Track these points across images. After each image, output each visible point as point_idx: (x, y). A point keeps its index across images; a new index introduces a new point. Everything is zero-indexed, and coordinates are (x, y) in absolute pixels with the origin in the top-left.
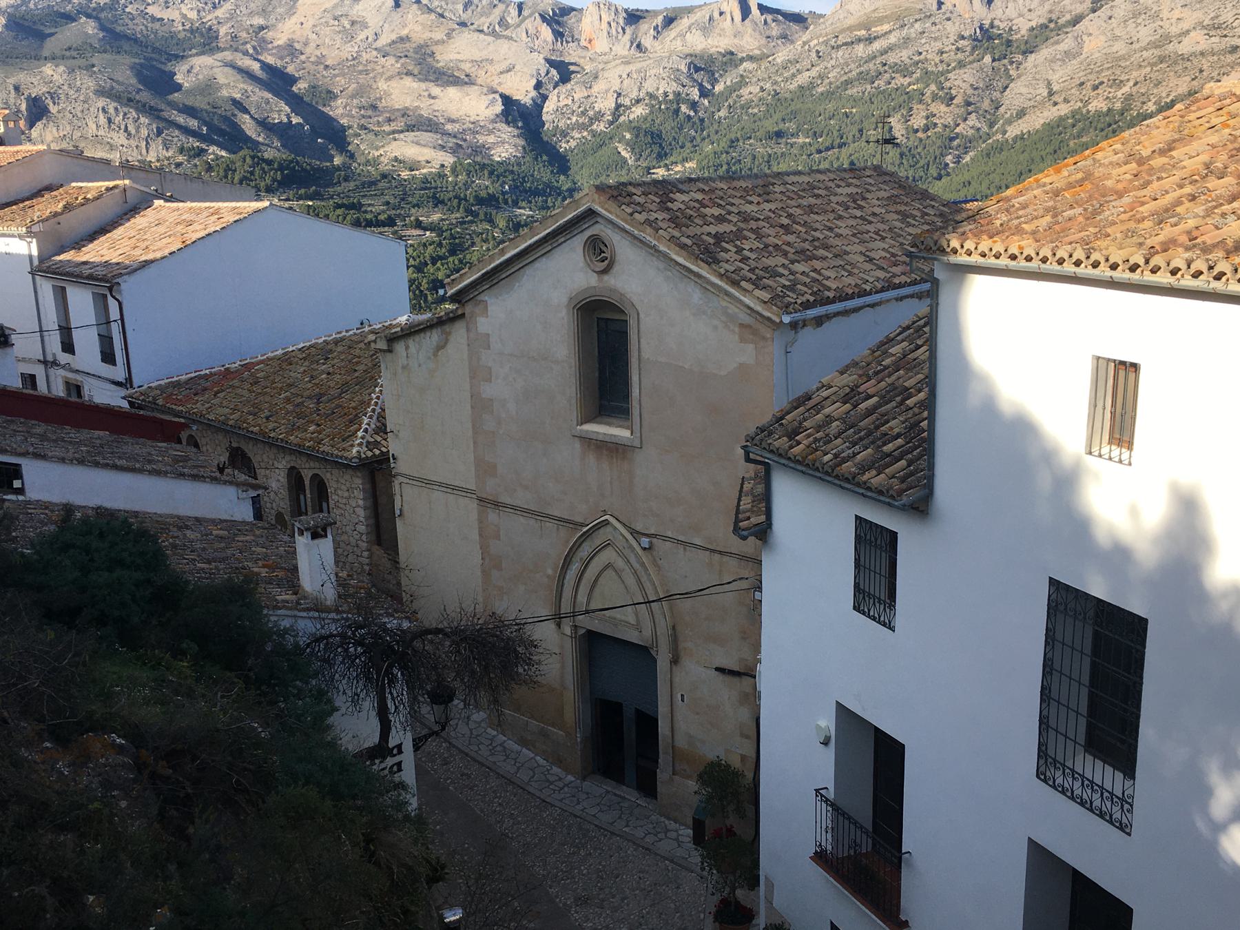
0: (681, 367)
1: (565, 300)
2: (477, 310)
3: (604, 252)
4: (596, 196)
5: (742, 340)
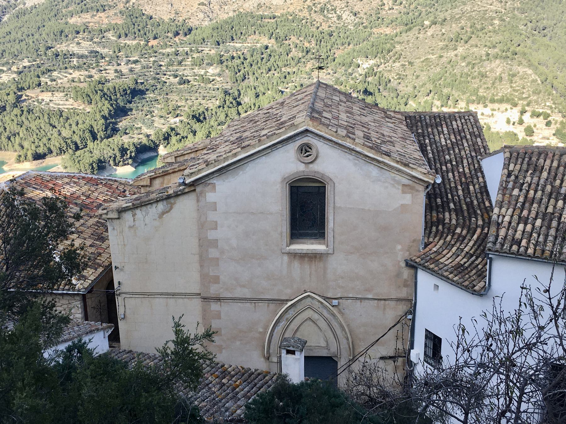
0: (363, 209)
1: (279, 179)
2: (207, 189)
4: (310, 123)
5: (404, 192)
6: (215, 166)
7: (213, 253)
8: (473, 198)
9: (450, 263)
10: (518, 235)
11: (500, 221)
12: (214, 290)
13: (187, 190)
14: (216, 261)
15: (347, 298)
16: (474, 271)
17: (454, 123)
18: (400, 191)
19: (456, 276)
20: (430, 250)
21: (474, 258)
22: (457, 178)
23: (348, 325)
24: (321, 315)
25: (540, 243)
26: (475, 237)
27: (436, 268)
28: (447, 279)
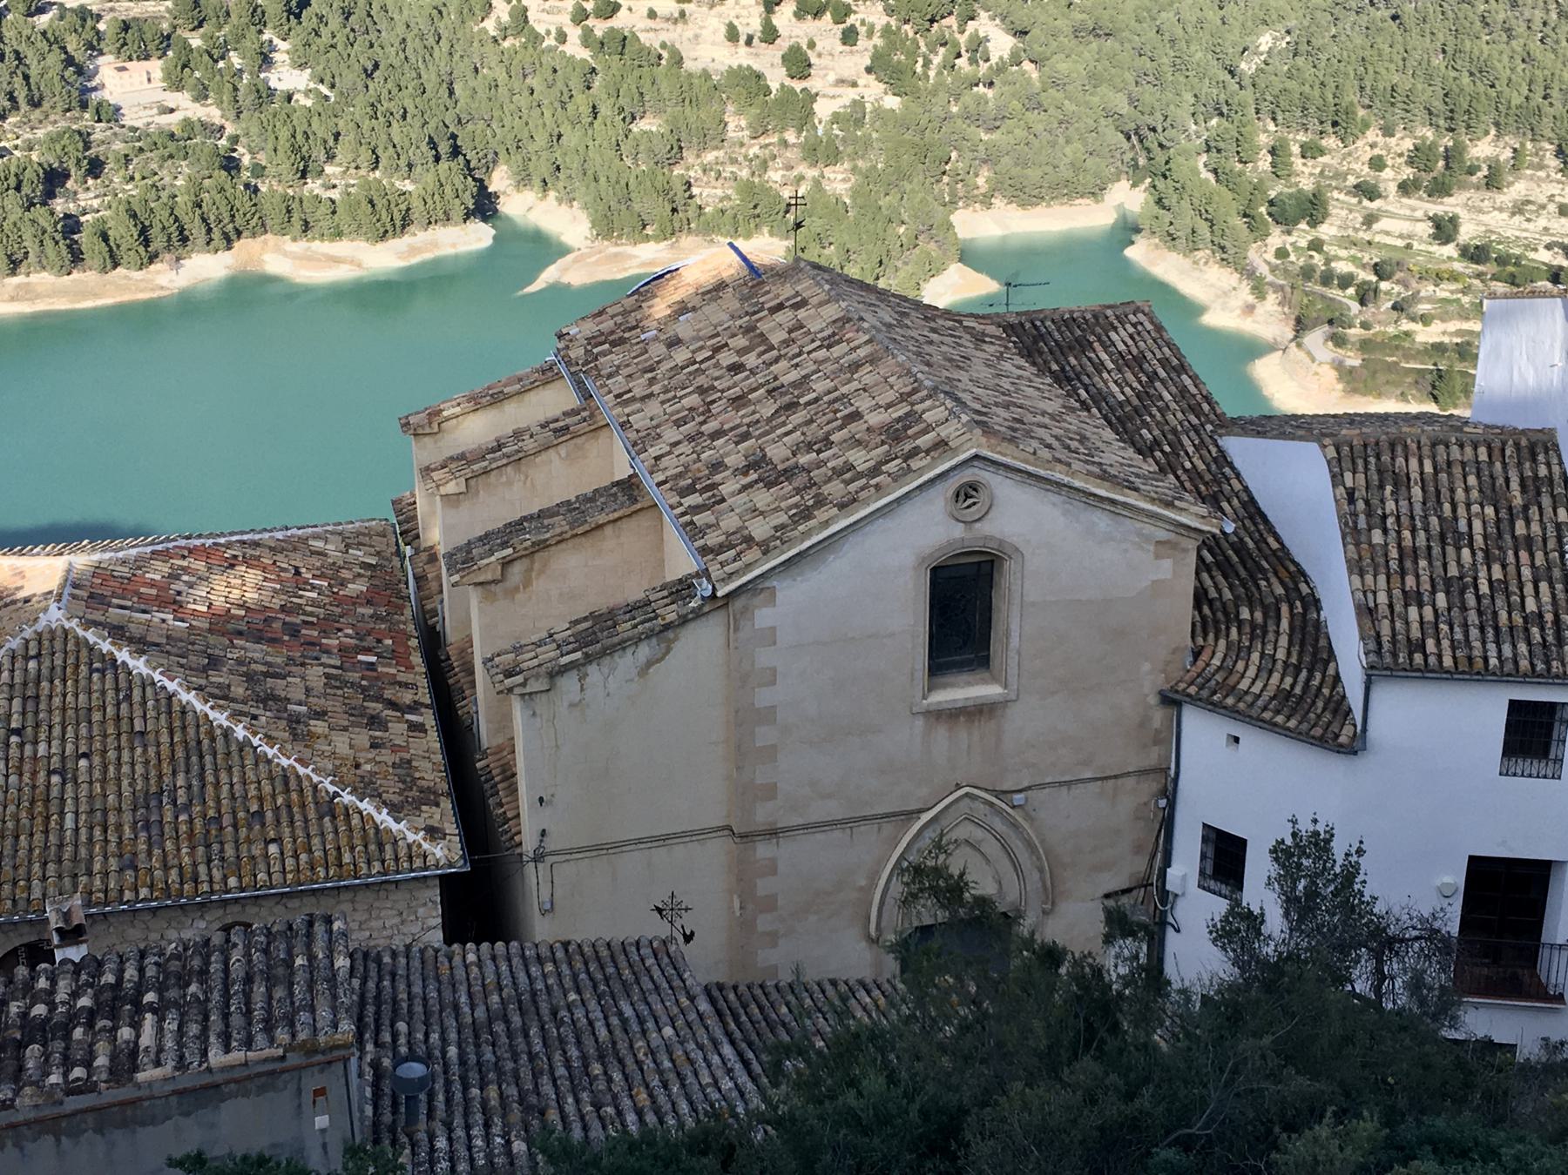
2: (757, 601)
3: (972, 497)
4: (984, 440)
5: (1158, 556)
7: (765, 735)
10: (1415, 633)
11: (1371, 604)
12: (763, 815)
13: (706, 609)
14: (770, 753)
15: (1042, 786)
16: (1320, 704)
17: (1113, 335)
18: (1152, 555)
19: (1288, 718)
20: (1208, 665)
21: (1304, 673)
23: (1042, 842)
24: (990, 830)
25: (1459, 642)
26: (1285, 624)
27: (1241, 705)
28: (1272, 727)
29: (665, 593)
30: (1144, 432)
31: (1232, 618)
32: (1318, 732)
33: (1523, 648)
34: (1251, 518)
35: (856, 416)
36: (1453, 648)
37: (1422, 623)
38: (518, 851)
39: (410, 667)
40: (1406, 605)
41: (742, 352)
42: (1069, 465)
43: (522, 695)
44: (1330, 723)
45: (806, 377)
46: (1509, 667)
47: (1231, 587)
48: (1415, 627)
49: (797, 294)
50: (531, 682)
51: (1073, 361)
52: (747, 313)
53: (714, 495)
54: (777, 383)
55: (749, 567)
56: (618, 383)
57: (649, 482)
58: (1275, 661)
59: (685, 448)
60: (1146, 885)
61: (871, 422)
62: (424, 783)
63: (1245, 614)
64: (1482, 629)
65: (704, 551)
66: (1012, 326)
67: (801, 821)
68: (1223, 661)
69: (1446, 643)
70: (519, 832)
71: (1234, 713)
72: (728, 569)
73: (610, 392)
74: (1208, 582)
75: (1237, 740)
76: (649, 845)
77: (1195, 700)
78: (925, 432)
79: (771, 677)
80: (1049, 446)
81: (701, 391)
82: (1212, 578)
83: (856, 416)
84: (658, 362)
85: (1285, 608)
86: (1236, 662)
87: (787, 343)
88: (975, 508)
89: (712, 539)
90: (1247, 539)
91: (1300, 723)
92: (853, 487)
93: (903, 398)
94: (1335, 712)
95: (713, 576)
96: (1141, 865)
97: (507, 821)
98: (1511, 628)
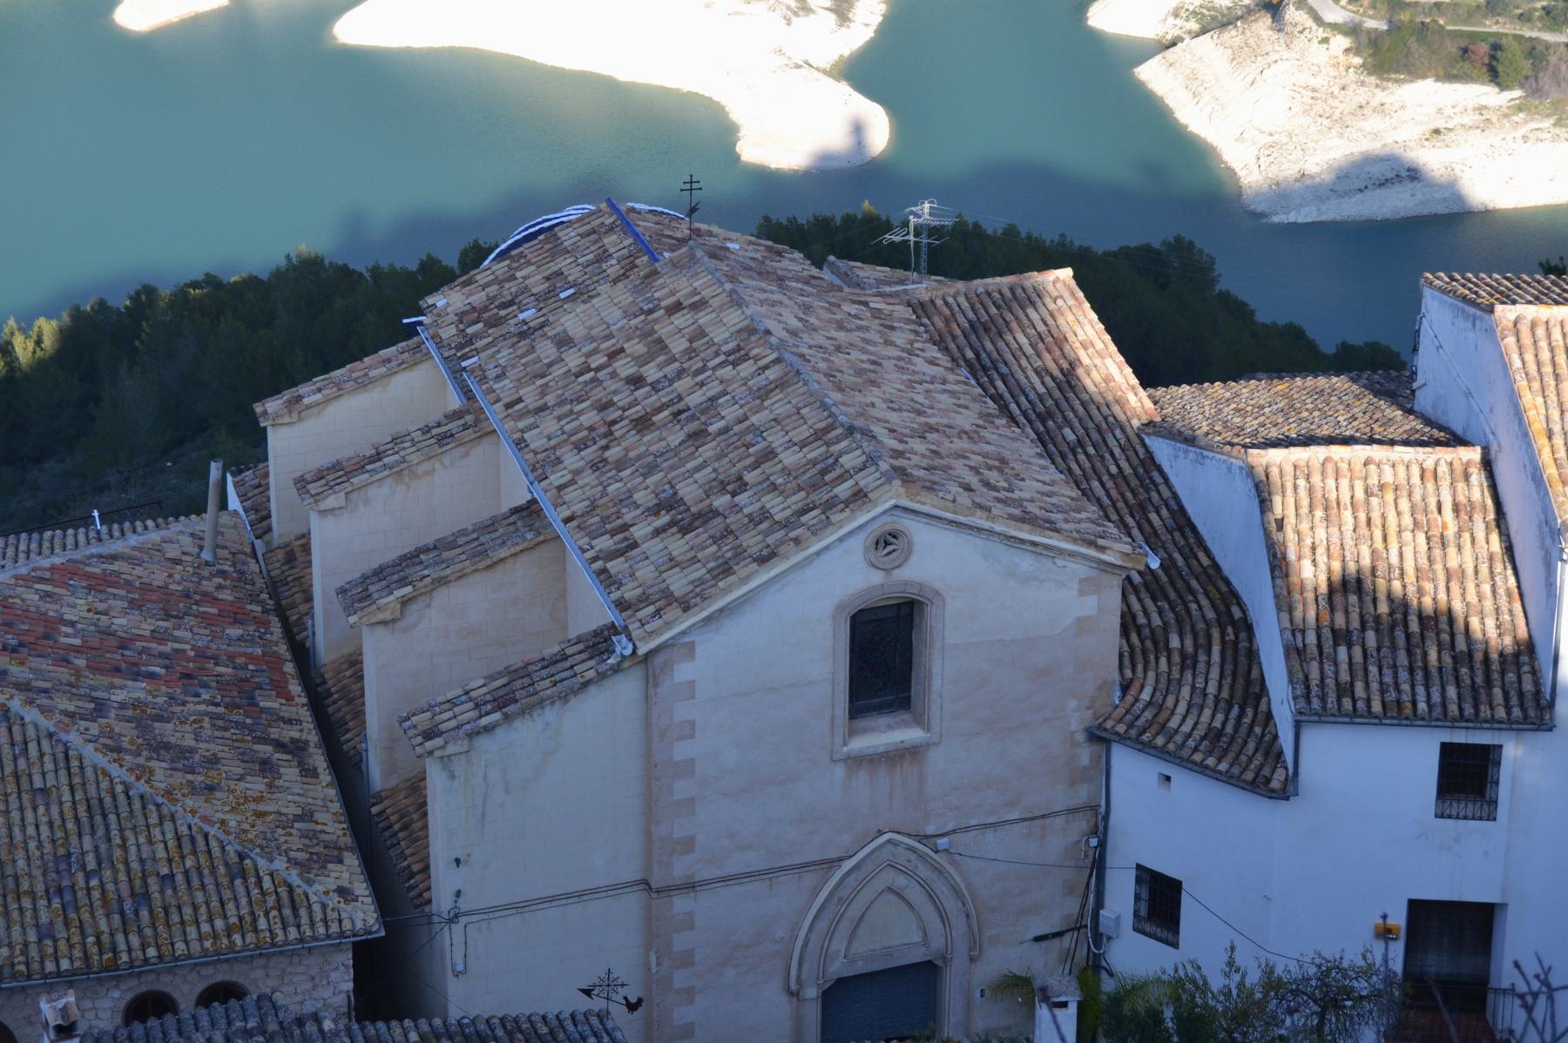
5: (1082, 593)
6: (703, 610)
7: (684, 788)
8: (1171, 547)
9: (1193, 729)
10: (1345, 677)
11: (1300, 645)
12: (681, 868)
15: (967, 829)
16: (1251, 745)
19: (1219, 760)
21: (1235, 711)
22: (1114, 493)
23: (968, 885)
24: (911, 874)
25: (1388, 685)
26: (1216, 649)
27: (1171, 746)
28: (1202, 769)
29: (581, 646)
30: (1067, 431)
31: (1159, 644)
32: (1249, 776)
33: (1452, 692)
34: (1181, 530)
35: (769, 454)
36: (1383, 692)
37: (1351, 663)
38: (427, 909)
39: (289, 698)
40: (1336, 644)
41: (642, 361)
42: (989, 510)
43: (442, 758)
44: (1262, 766)
45: (712, 399)
46: (1438, 711)
47: (1160, 612)
48: (1344, 667)
49: (695, 292)
50: (450, 745)
51: (989, 346)
52: (642, 311)
53: (626, 539)
54: (681, 406)
55: (668, 625)
56: (505, 388)
57: (554, 516)
58: (1205, 695)
59: (588, 478)
60: (1078, 927)
61: (786, 462)
62: (327, 837)
63: (1175, 642)
64: (1411, 670)
65: (622, 605)
66: (922, 304)
67: (719, 873)
68: (1153, 696)
69: (1375, 686)
70: (429, 888)
71: (1162, 754)
72: (647, 627)
73: (498, 400)
74: (1136, 606)
75: (1168, 778)
76: (564, 902)
77: (1123, 739)
78: (841, 479)
79: (690, 730)
80: (968, 488)
81: (603, 407)
82: (1140, 600)
83: (769, 454)
84: (550, 365)
85: (1216, 634)
86: (1165, 697)
87: (690, 353)
88: (894, 555)
89: (630, 592)
90: (1177, 555)
91: (1231, 765)
92: (770, 540)
93: (818, 435)
94: (1267, 754)
95: (634, 634)
96: (1072, 906)
97: (412, 875)
98: (1440, 669)
